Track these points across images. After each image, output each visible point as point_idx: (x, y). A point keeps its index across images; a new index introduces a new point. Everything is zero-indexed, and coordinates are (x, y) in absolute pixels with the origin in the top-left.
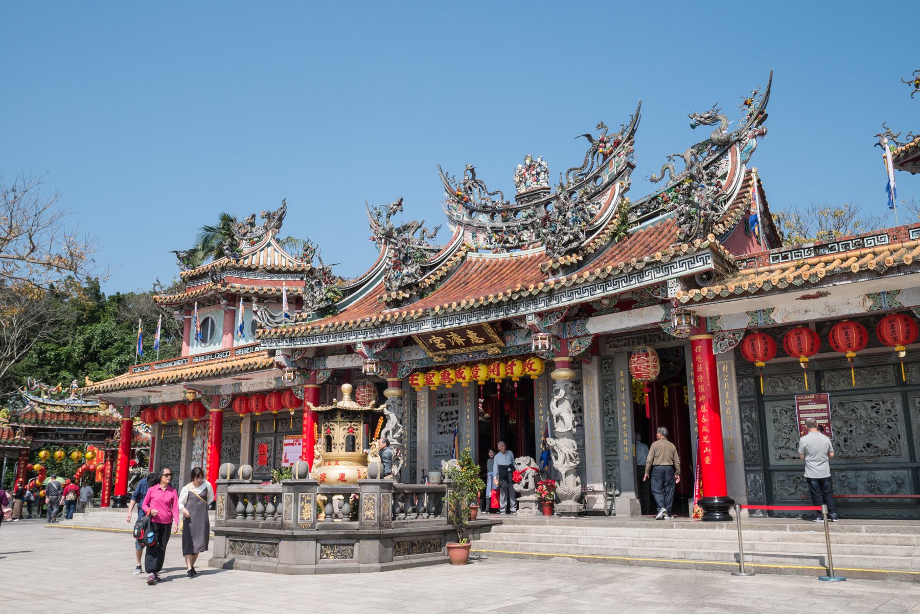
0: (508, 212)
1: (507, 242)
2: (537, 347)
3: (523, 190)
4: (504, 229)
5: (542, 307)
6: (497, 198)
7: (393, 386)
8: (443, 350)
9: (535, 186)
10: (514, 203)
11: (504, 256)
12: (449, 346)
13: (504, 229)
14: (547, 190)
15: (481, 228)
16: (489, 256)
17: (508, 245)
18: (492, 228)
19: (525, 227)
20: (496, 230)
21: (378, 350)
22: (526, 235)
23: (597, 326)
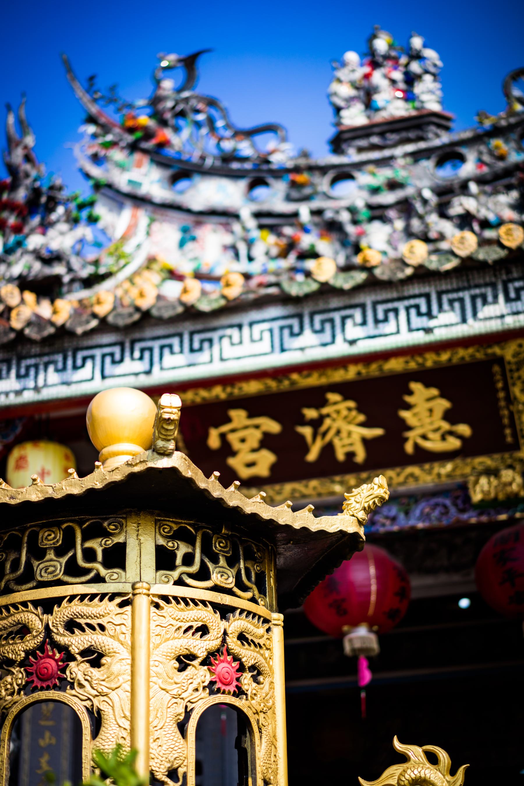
3: (355, 117)
9: (399, 109)
15: (226, 216)
18: (258, 215)
19: (378, 213)
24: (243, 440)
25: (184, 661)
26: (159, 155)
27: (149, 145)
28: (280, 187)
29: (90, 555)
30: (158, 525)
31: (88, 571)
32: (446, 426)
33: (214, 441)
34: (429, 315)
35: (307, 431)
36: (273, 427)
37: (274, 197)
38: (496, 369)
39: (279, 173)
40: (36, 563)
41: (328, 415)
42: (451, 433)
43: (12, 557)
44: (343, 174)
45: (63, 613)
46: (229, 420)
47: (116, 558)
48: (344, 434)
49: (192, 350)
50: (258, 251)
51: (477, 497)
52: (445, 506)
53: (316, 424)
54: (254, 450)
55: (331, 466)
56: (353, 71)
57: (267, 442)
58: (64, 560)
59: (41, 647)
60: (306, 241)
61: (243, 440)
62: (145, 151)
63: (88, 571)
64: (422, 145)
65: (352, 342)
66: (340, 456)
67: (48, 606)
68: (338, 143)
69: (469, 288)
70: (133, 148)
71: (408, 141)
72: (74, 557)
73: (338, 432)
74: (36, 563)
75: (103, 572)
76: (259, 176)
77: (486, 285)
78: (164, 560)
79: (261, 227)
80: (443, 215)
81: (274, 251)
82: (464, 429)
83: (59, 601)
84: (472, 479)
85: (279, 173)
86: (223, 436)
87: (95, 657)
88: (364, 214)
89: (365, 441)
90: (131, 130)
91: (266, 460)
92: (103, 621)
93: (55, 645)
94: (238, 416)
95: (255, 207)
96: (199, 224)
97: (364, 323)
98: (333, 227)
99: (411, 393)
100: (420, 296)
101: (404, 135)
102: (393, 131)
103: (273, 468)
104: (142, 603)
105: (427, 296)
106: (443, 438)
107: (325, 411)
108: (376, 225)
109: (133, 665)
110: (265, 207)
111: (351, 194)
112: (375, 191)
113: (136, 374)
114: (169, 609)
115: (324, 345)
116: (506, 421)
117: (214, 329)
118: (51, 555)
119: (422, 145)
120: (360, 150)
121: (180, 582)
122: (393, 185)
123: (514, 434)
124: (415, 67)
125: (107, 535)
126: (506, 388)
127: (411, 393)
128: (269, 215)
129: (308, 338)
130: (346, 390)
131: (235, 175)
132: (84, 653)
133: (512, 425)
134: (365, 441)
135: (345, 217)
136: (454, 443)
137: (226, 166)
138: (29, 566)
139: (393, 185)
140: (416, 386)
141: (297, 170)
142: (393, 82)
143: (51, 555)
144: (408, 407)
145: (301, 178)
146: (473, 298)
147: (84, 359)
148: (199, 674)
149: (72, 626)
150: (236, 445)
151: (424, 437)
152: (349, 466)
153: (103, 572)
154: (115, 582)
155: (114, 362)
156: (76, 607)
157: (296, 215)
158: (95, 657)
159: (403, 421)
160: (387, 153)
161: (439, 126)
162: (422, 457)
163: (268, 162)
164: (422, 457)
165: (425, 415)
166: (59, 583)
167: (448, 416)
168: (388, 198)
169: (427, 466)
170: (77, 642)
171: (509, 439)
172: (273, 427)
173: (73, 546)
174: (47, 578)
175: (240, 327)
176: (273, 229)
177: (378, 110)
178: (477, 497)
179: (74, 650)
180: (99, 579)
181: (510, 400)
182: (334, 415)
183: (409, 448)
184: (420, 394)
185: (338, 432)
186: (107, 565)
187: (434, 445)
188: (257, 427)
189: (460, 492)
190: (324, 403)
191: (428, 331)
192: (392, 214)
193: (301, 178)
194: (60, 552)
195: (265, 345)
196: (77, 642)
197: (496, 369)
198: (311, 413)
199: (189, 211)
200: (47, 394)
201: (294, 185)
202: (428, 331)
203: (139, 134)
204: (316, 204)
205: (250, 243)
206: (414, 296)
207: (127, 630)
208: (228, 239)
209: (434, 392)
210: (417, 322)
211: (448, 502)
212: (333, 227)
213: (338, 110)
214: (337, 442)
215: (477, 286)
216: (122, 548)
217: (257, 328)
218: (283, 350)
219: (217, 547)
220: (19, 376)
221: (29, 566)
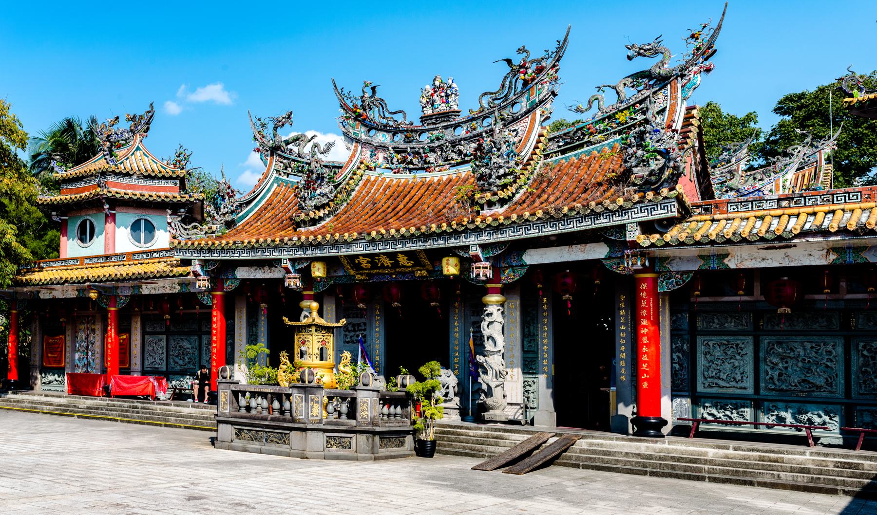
0: (410, 133)
1: (411, 163)
3: (429, 111)
4: (409, 150)
6: (399, 118)
8: (367, 269)
10: (417, 123)
11: (405, 177)
12: (374, 265)
13: (409, 150)
15: (383, 147)
16: (389, 175)
17: (411, 166)
19: (432, 150)
20: (398, 151)
21: (302, 266)
22: (432, 157)
23: (532, 258)
50: (395, 161)
68: (423, 119)
76: (395, 131)
80: (453, 151)
94: (361, 258)
112: (432, 141)
120: (428, 124)
122: (438, 139)
129: (371, 248)
135: (421, 150)
139: (438, 139)
141: (407, 131)
187: (406, 264)
192: (437, 150)
201: (406, 136)
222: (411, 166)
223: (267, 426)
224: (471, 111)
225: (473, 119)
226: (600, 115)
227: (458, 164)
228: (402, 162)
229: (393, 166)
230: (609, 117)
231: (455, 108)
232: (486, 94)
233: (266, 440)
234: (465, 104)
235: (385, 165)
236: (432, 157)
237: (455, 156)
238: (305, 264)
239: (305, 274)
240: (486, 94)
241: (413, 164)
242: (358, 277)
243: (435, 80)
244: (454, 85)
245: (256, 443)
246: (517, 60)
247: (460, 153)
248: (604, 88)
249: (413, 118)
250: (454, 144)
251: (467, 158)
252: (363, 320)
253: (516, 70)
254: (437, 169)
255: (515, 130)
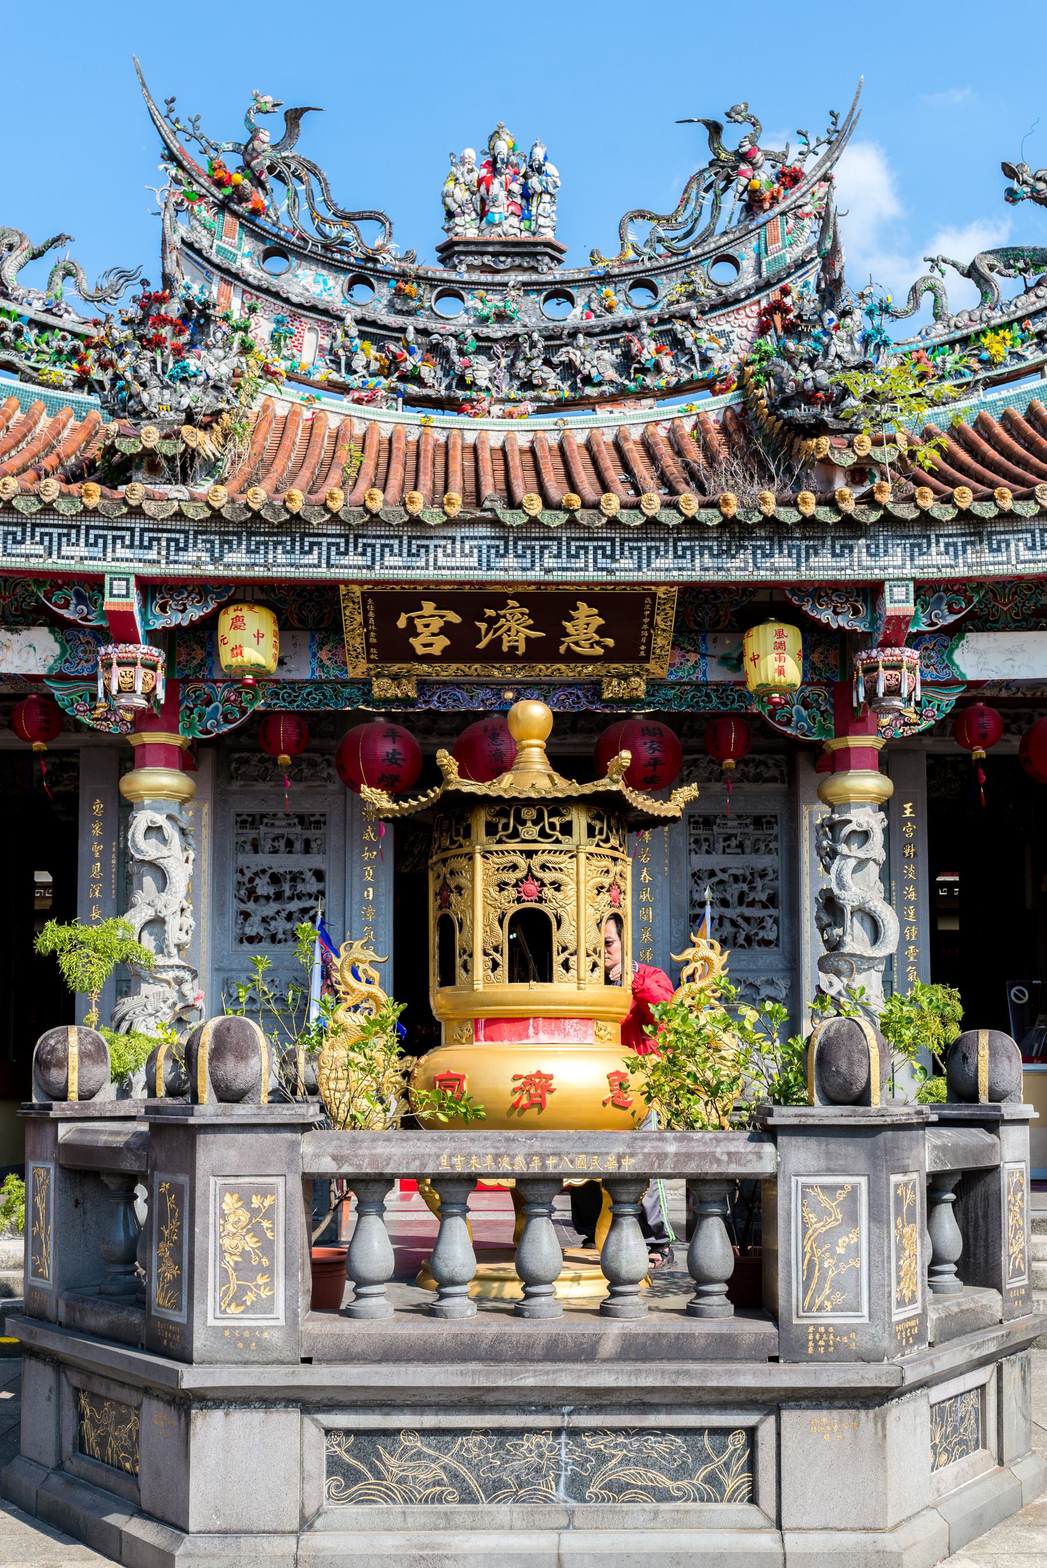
1: (417, 379)
2: (871, 693)
3: (468, 229)
4: (411, 335)
5: (939, 561)
6: (372, 236)
7: (168, 764)
9: (511, 228)
12: (462, 645)
13: (411, 335)
14: (554, 252)
17: (413, 389)
18: (360, 321)
19: (485, 347)
20: (372, 331)
21: (174, 618)
22: (482, 370)
24: (427, 626)
25: (600, 889)
26: (251, 223)
27: (243, 208)
28: (384, 291)
29: (552, 826)
30: (588, 810)
31: (551, 836)
32: (597, 638)
33: (402, 623)
34: (612, 557)
35: (483, 626)
36: (454, 618)
37: (376, 302)
38: (648, 600)
39: (385, 276)
40: (520, 828)
41: (504, 616)
42: (598, 643)
43: (504, 821)
44: (451, 291)
45: (537, 861)
46: (421, 609)
47: (567, 829)
48: (513, 632)
49: (410, 554)
50: (358, 363)
51: (607, 695)
52: (578, 697)
53: (491, 621)
54: (433, 635)
55: (495, 654)
56: (471, 171)
57: (447, 629)
58: (538, 828)
59: (526, 878)
60: (410, 363)
61: (427, 626)
62: (235, 214)
63: (551, 836)
64: (535, 277)
65: (548, 571)
66: (505, 649)
67: (529, 854)
68: (448, 252)
69: (646, 540)
70: (223, 206)
71: (520, 268)
72: (543, 827)
73: (509, 630)
74: (520, 828)
75: (560, 837)
76: (363, 274)
77: (661, 540)
78: (591, 833)
79: (363, 335)
81: (375, 366)
82: (610, 642)
83: (536, 852)
84: (606, 680)
85: (385, 276)
86: (410, 620)
87: (557, 887)
88: (471, 345)
89: (528, 639)
90: (220, 184)
91: (442, 642)
92: (562, 866)
93: (534, 877)
94: (429, 607)
95: (358, 312)
96: (294, 317)
97: (558, 556)
98: (437, 351)
99: (576, 609)
100: (606, 539)
101: (518, 261)
102: (506, 254)
103: (445, 650)
104: (582, 857)
105: (612, 540)
106: (592, 647)
107: (501, 613)
108: (482, 359)
109: (578, 892)
110: (370, 316)
111: (457, 317)
112: (483, 320)
113: (359, 568)
114: (594, 861)
115: (524, 569)
116: (644, 640)
117: (431, 538)
118: (529, 824)
119: (535, 277)
120: (471, 268)
121: (598, 845)
122: (501, 317)
123: (647, 652)
124: (534, 182)
125: (562, 815)
126: (651, 616)
127: (576, 609)
128: (373, 324)
129: (511, 561)
130: (523, 599)
131: (337, 268)
132: (551, 884)
133: (648, 644)
134: (528, 639)
135: (452, 344)
136: (599, 651)
137: (327, 256)
138: (515, 829)
139: (501, 317)
140: (582, 605)
142: (510, 192)
143: (529, 824)
144: (571, 619)
145: (411, 288)
146: (649, 548)
147: (312, 545)
148: (606, 897)
149: (543, 867)
150: (420, 629)
151: (577, 644)
152: (511, 656)
153: (560, 837)
154: (568, 843)
155: (339, 553)
156: (546, 857)
157: (403, 330)
158: (557, 887)
159: (565, 628)
160: (498, 278)
161: (553, 258)
162: (572, 657)
163: (376, 261)
164: (572, 657)
165: (584, 626)
166: (535, 841)
167: (600, 631)
168: (496, 331)
169: (572, 665)
170: (548, 876)
171: (642, 654)
172: (454, 618)
173: (543, 820)
174: (528, 837)
175: (453, 539)
176: (376, 340)
177: (492, 224)
178: (607, 695)
179: (546, 882)
180: (558, 841)
181: (652, 625)
182: (509, 617)
183: (562, 649)
184: (583, 609)
185: (509, 630)
186: (563, 833)
187: (585, 650)
188: (442, 617)
189: (595, 687)
190: (505, 605)
191: (611, 571)
192: (498, 349)
193: (411, 288)
194: (535, 823)
195: (473, 562)
196: (548, 876)
197: (648, 600)
198: (490, 613)
199: (287, 301)
200: (277, 572)
201: (399, 293)
202: (611, 571)
203: (228, 191)
204: (422, 322)
205: (351, 353)
206: (602, 539)
207: (574, 872)
208: (326, 342)
209: (595, 611)
210: (602, 562)
211: (580, 693)
212: (437, 351)
213: (450, 215)
214: (505, 637)
215: (653, 539)
216: (570, 823)
217: (468, 544)
218: (489, 568)
219: (613, 822)
220: (249, 551)
221: (515, 829)
222: (413, 389)
223: (598, 1399)
224: (594, 257)
225: (606, 279)
226: (940, 333)
227: (562, 405)
228: (385, 372)
229: (354, 381)
230: (965, 341)
231: (549, 235)
232: (642, 215)
233: (577, 1487)
234: (584, 228)
235: (322, 373)
236: (482, 370)
237: (552, 377)
238: (195, 613)
239: (190, 650)
240: (642, 215)
241: (420, 381)
242: (383, 688)
243: (495, 135)
244: (549, 168)
245: (503, 1511)
246: (733, 139)
247: (569, 370)
248: (944, 266)
249: (410, 241)
250: (556, 339)
251: (589, 391)
252: (315, 861)
253: (727, 167)
254: (496, 409)
255: (722, 334)
